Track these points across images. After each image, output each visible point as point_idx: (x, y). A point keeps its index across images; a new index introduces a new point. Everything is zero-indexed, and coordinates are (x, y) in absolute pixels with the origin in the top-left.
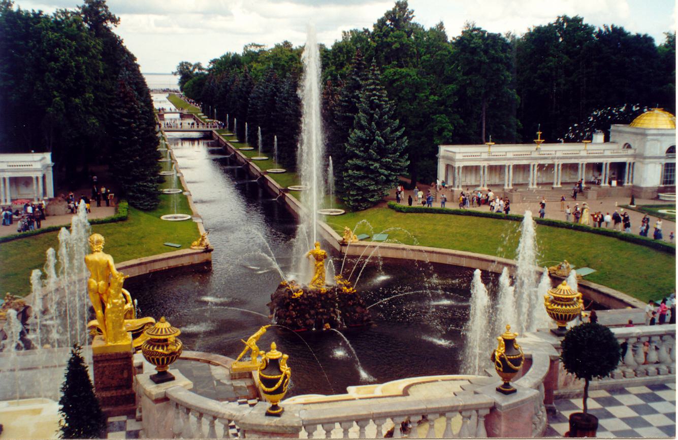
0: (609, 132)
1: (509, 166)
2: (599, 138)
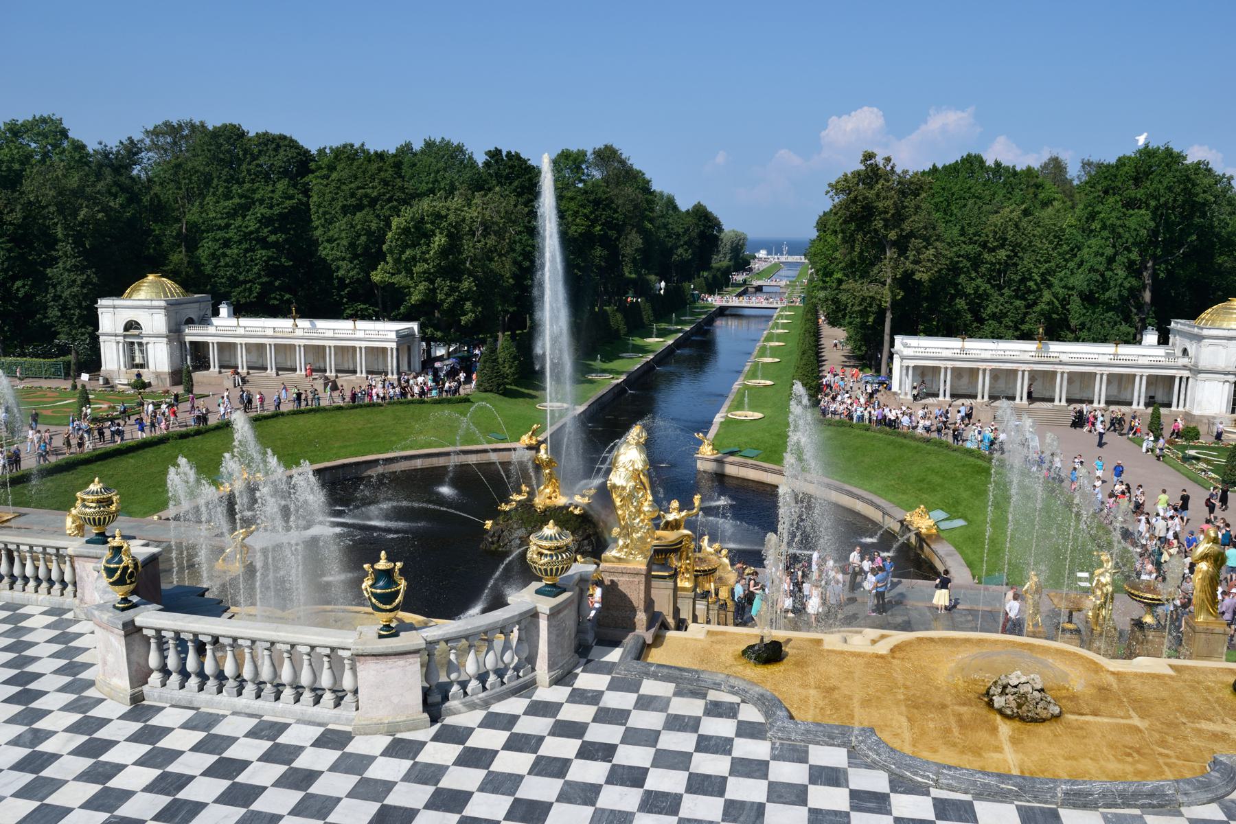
0: (1168, 331)
1: (984, 370)
2: (1151, 337)
